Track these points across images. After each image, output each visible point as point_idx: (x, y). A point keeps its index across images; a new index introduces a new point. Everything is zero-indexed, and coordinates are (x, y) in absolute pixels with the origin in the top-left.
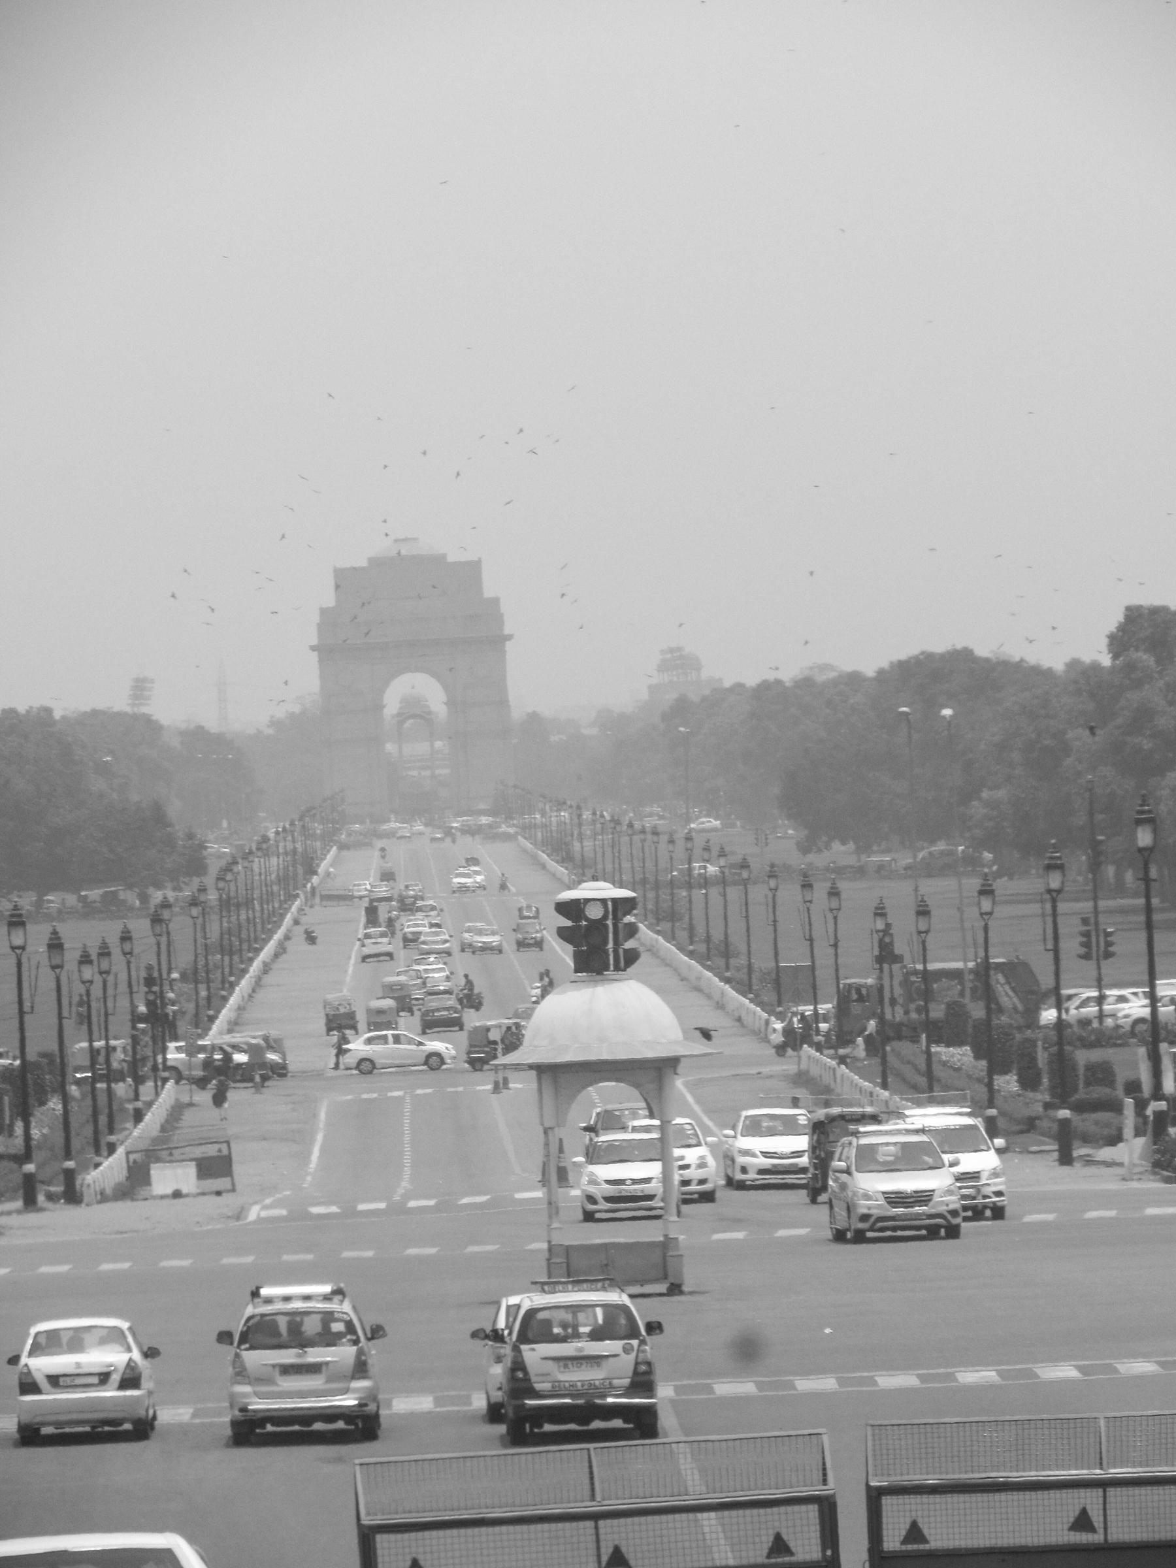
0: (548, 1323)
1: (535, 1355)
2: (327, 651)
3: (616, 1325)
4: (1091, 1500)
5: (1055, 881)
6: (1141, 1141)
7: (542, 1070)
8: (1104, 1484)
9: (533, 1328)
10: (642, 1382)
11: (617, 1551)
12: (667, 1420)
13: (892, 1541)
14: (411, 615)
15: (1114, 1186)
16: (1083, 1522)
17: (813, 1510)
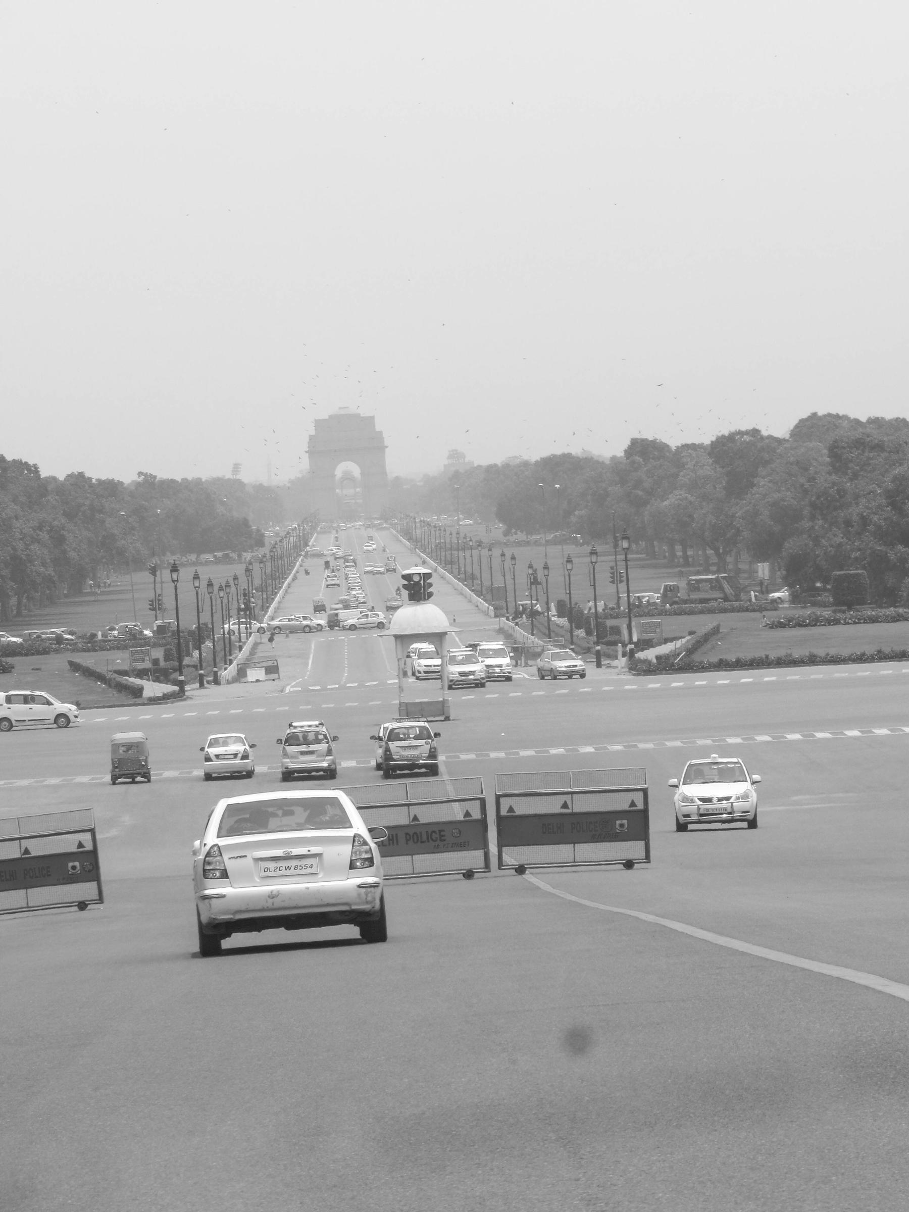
0: (398, 734)
1: (393, 745)
3: (424, 734)
4: (568, 798)
5: (594, 560)
6: (625, 659)
8: (572, 793)
9: (393, 736)
10: (433, 755)
11: (415, 816)
12: (442, 769)
13: (504, 812)
14: (346, 437)
15: (615, 677)
16: (565, 806)
17: (478, 802)
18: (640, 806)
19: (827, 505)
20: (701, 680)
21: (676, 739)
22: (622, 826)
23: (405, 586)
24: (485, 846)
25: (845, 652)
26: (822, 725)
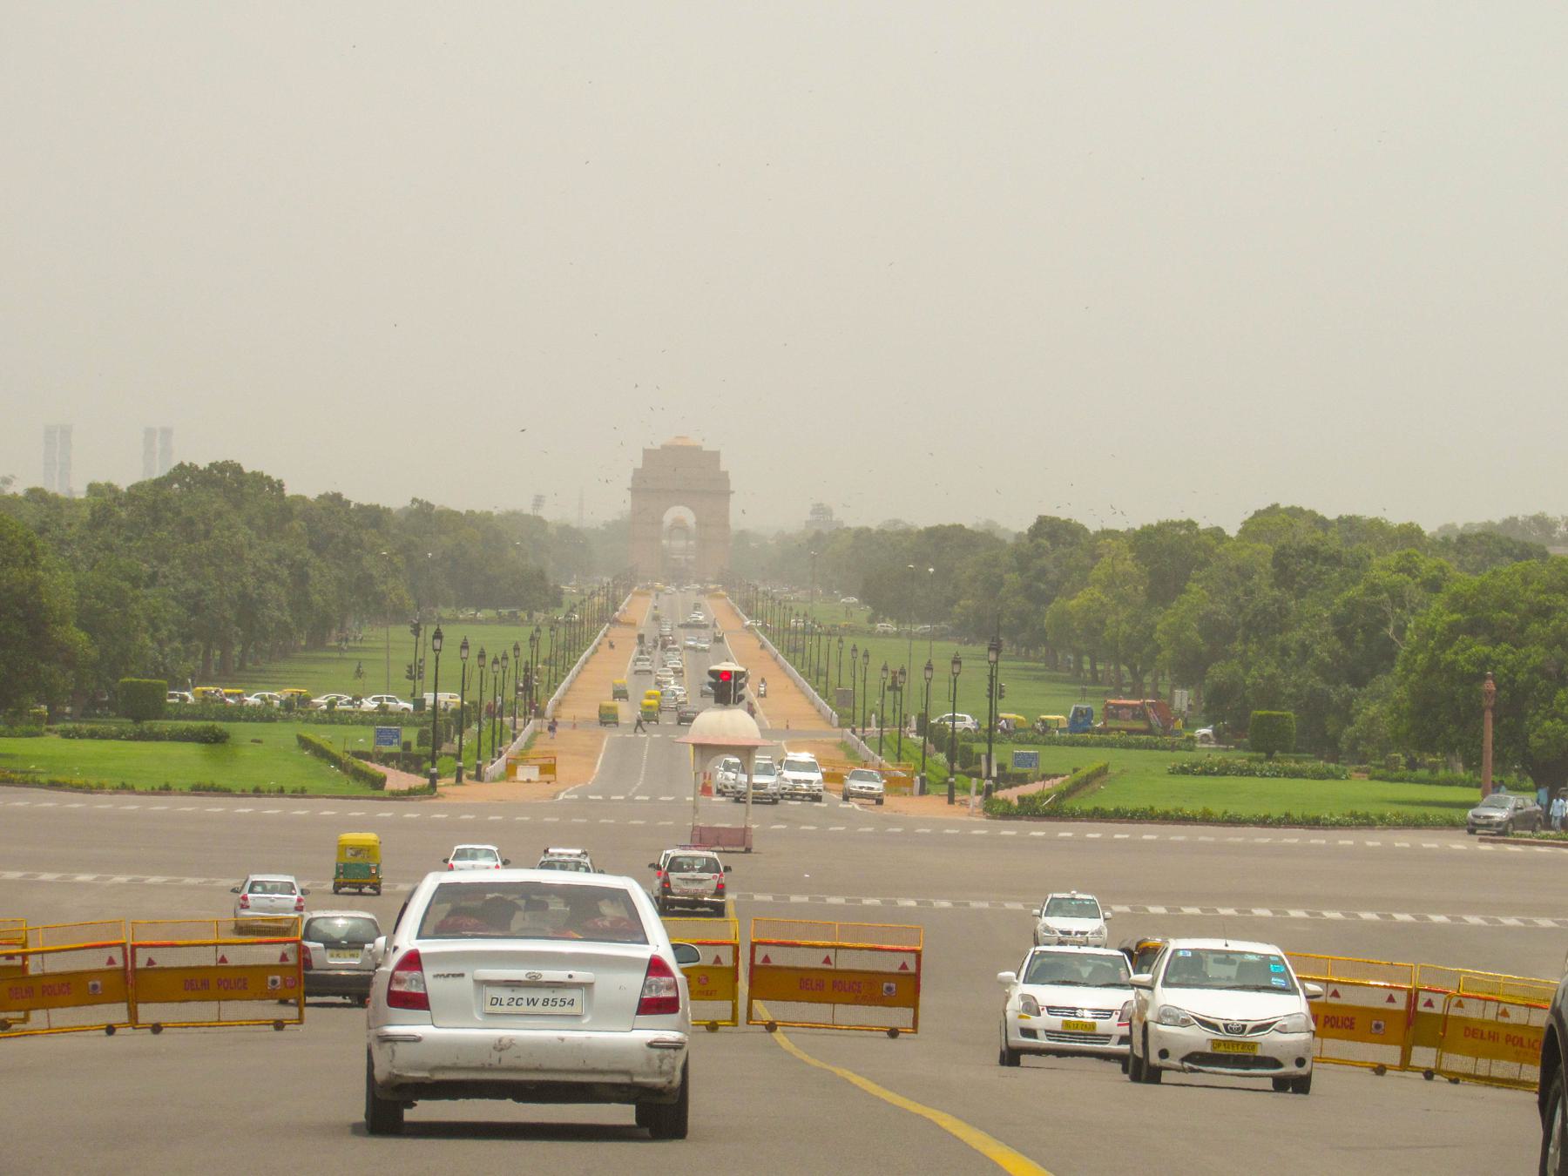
1: (673, 876)
2: (635, 491)
4: (831, 953)
6: (978, 798)
7: (695, 745)
9: (675, 865)
10: (720, 890)
12: (730, 909)
13: (758, 961)
14: (681, 476)
15: (965, 819)
16: (827, 961)
17: (730, 948)
18: (912, 968)
19: (1266, 625)
20: (1065, 831)
21: (983, 900)
22: (889, 989)
23: (710, 684)
24: (733, 996)
25: (1245, 812)
26: (1190, 898)
